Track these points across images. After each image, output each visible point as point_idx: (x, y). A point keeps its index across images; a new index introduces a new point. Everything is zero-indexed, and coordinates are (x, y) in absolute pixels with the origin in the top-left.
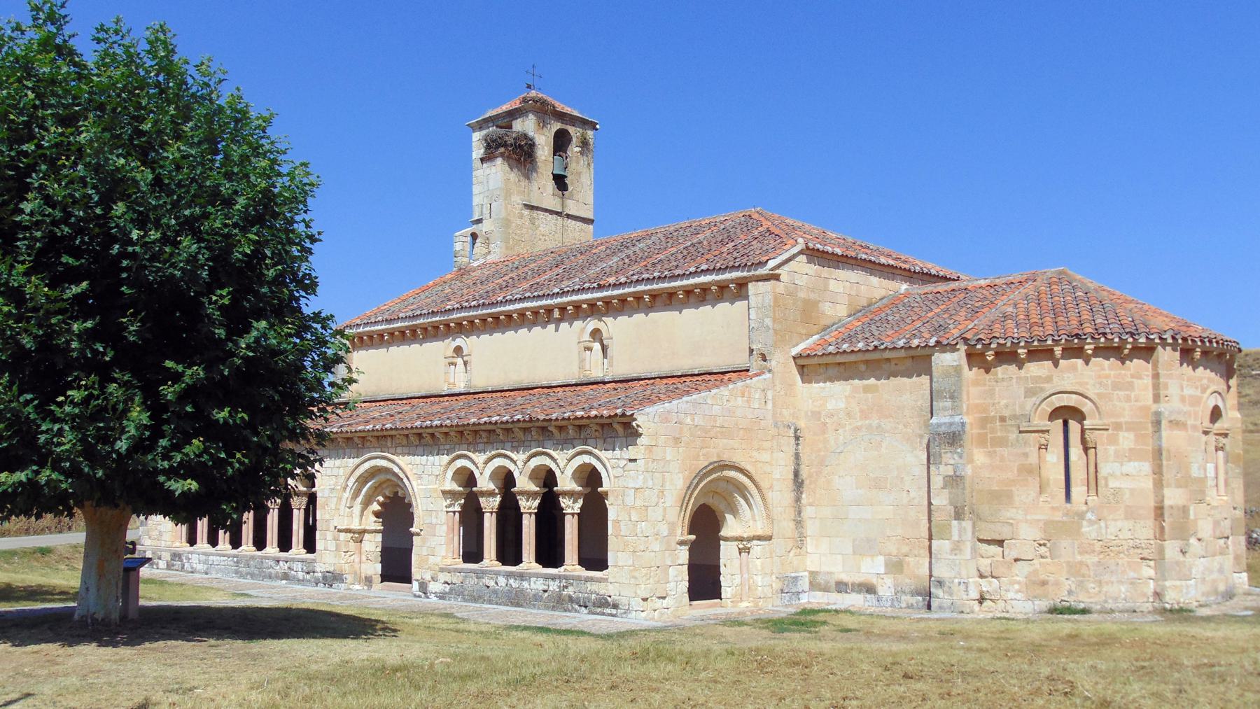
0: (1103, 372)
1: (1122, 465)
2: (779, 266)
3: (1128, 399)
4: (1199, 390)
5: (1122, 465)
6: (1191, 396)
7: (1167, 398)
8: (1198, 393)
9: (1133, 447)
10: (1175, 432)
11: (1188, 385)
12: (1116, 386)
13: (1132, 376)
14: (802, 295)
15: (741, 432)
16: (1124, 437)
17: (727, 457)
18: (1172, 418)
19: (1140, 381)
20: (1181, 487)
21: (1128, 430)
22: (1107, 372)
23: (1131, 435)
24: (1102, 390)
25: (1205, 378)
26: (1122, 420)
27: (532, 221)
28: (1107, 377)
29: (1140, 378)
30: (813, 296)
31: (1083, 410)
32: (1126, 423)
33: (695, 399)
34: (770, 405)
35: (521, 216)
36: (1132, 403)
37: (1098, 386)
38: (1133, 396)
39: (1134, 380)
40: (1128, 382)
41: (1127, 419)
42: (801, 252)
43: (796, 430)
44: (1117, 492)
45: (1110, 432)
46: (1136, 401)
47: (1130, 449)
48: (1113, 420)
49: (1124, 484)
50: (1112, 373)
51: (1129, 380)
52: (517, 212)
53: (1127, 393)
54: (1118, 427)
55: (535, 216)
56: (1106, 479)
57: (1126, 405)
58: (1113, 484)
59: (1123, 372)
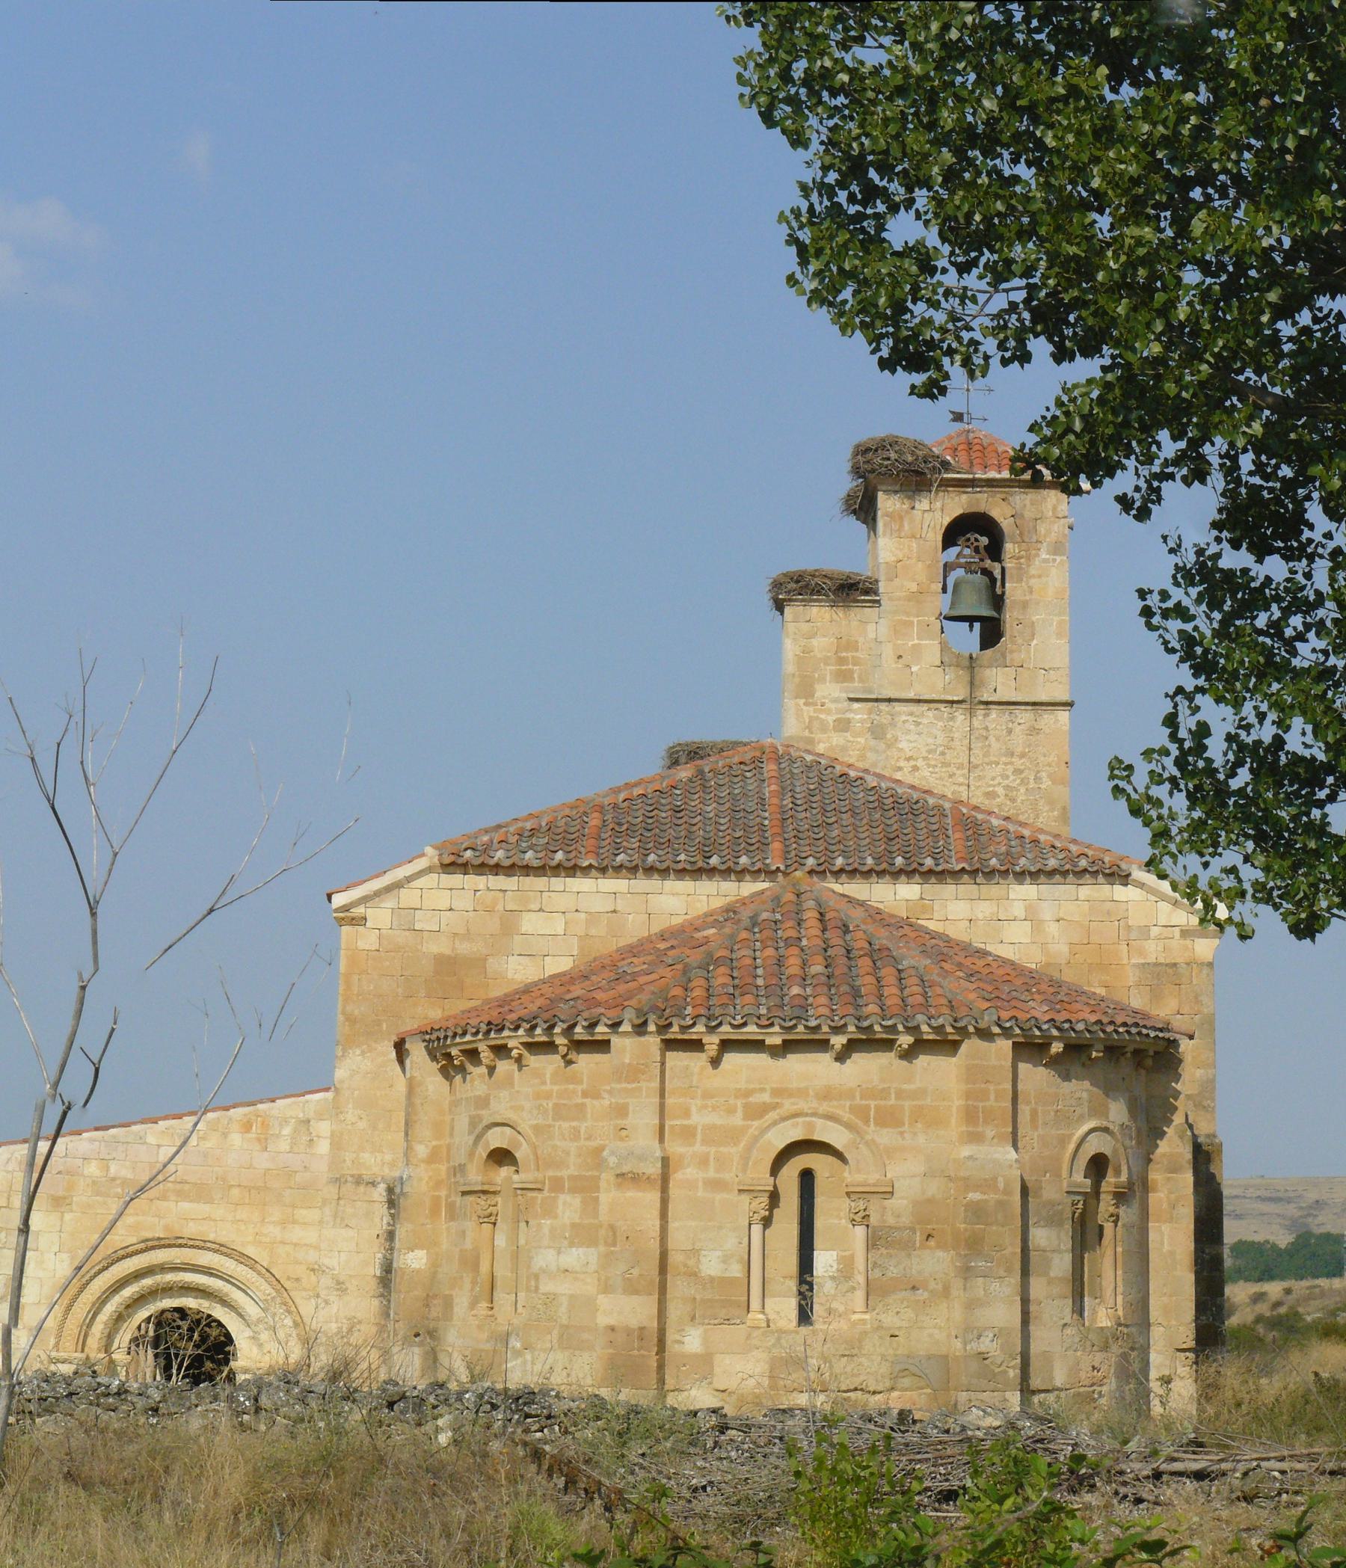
0: (543, 1087)
1: (559, 1253)
2: (364, 900)
3: (576, 1135)
4: (740, 1113)
5: (559, 1253)
6: (711, 1128)
7: (624, 1133)
8: (737, 1120)
9: (577, 1221)
10: (629, 1194)
11: (705, 1107)
12: (559, 1113)
13: (585, 1094)
14: (439, 947)
15: (235, 1192)
16: (564, 1203)
17: (191, 1230)
18: (625, 1169)
19: (595, 1102)
20: (636, 1292)
21: (573, 1190)
22: (548, 1087)
23: (576, 1201)
24: (540, 1121)
25: (763, 1090)
26: (565, 1173)
27: (877, 732)
28: (548, 1096)
29: (597, 1096)
30: (464, 948)
31: (517, 1155)
32: (572, 1178)
33: (114, 1137)
34: (323, 1147)
35: (843, 725)
36: (582, 1142)
37: (535, 1112)
38: (582, 1131)
39: (587, 1101)
40: (577, 1105)
41: (572, 1171)
42: (429, 870)
43: (390, 1190)
44: (551, 1299)
45: (546, 1193)
46: (587, 1139)
47: (573, 1225)
48: (550, 1173)
49: (562, 1288)
50: (556, 1088)
51: (580, 1101)
52: (830, 719)
53: (574, 1124)
54: (557, 1185)
55: (885, 720)
56: (537, 1277)
57: (572, 1147)
58: (547, 1286)
59: (571, 1087)
